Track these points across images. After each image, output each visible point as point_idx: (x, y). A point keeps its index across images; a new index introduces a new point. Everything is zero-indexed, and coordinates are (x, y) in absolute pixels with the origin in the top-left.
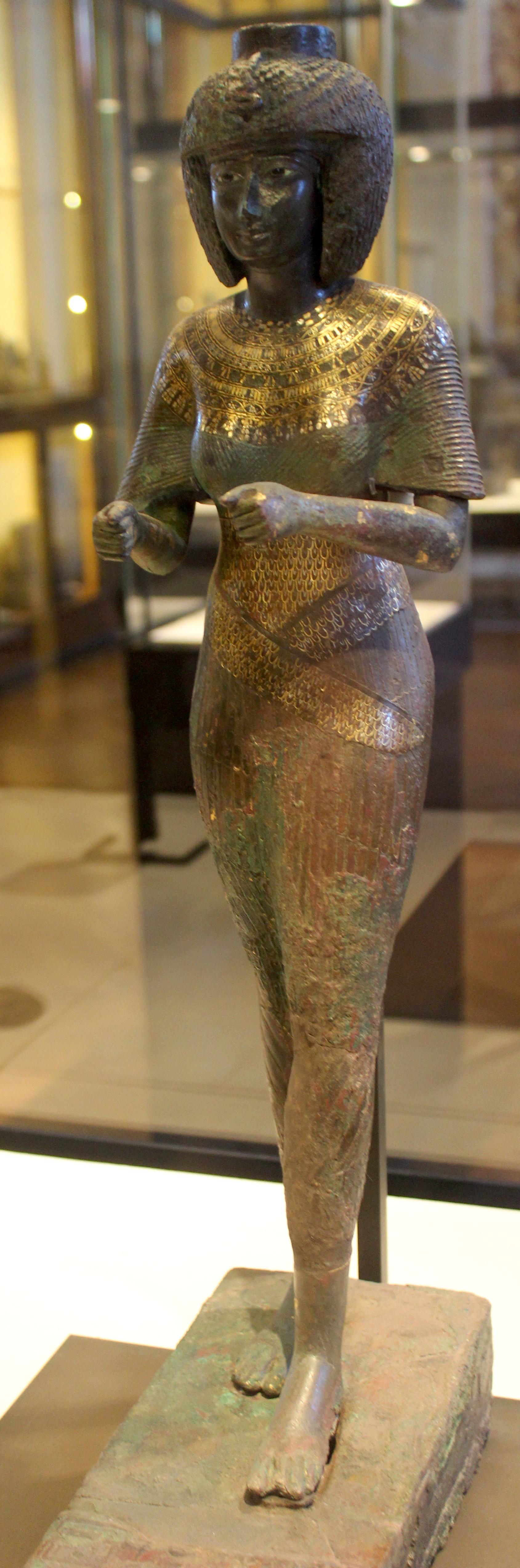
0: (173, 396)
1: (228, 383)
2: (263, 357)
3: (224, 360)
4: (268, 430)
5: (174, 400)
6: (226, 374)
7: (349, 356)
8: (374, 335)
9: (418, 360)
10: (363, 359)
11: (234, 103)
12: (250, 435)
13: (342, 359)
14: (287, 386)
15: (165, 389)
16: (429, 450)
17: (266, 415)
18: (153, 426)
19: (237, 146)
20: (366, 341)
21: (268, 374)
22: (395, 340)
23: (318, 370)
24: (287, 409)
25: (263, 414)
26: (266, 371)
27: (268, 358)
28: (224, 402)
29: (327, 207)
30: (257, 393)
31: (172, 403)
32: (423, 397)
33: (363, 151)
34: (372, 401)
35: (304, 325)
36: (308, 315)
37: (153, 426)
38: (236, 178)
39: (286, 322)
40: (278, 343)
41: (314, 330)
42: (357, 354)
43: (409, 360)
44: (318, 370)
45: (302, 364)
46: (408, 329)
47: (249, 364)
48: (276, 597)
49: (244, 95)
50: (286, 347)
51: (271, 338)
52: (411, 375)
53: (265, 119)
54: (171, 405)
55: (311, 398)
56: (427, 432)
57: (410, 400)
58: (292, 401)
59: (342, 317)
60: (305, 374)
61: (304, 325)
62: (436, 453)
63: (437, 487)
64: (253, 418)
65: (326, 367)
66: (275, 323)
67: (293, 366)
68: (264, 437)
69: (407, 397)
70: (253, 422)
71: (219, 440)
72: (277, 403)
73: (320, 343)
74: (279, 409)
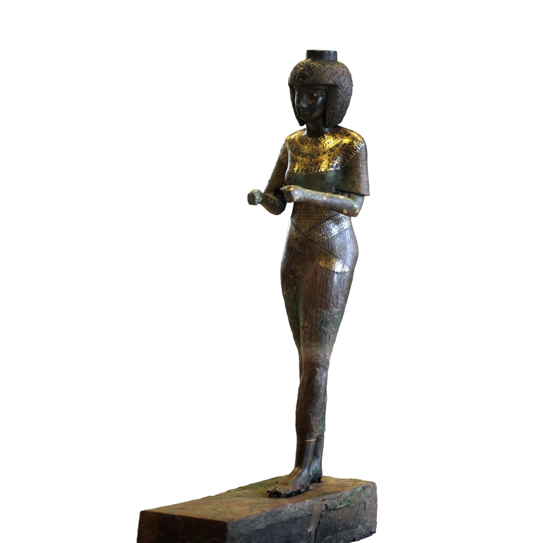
7: (331, 150)
14: (313, 158)
20: (337, 145)
21: (309, 154)
29: (327, 105)
30: (304, 159)
41: (323, 141)
48: (306, 222)
49: (303, 72)
56: (352, 174)
59: (332, 138)
60: (318, 155)
63: (352, 191)
65: (325, 153)
67: (316, 152)
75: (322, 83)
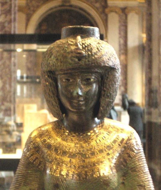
0: (34, 159)
1: (62, 156)
2: (75, 146)
3: (59, 147)
4: (79, 175)
5: (35, 161)
6: (60, 153)
8: (117, 140)
9: (133, 149)
10: (114, 148)
11: (75, 54)
12: (72, 177)
13: (107, 148)
14: (86, 158)
15: (30, 156)
16: (139, 183)
17: (78, 169)
18: (25, 171)
19: (73, 69)
20: (115, 141)
21: (78, 153)
22: (125, 142)
23: (98, 153)
24: (87, 167)
25: (77, 169)
26: (77, 152)
27: (77, 147)
28: (61, 164)
29: (103, 92)
30: (73, 160)
31: (33, 162)
32: (135, 163)
33: (116, 73)
34: (118, 164)
35: (91, 135)
36: (92, 131)
37: (25, 171)
38: (71, 81)
39: (84, 133)
40: (81, 141)
41: (95, 137)
42: (112, 147)
43: (130, 149)
44: (98, 153)
45: (91, 150)
46: (129, 137)
47: (70, 149)
50: (84, 143)
51: (78, 140)
52: (131, 155)
53: (87, 60)
54: (33, 163)
55: (96, 163)
56: (138, 176)
57: (131, 164)
58: (89, 164)
60: (93, 154)
61: (91, 135)
62: (142, 184)
64: (73, 170)
66: (79, 134)
68: (78, 178)
69: (130, 163)
70: (73, 172)
71: (61, 179)
72: (82, 164)
73: (98, 142)
74: (83, 167)
75: (103, 64)
